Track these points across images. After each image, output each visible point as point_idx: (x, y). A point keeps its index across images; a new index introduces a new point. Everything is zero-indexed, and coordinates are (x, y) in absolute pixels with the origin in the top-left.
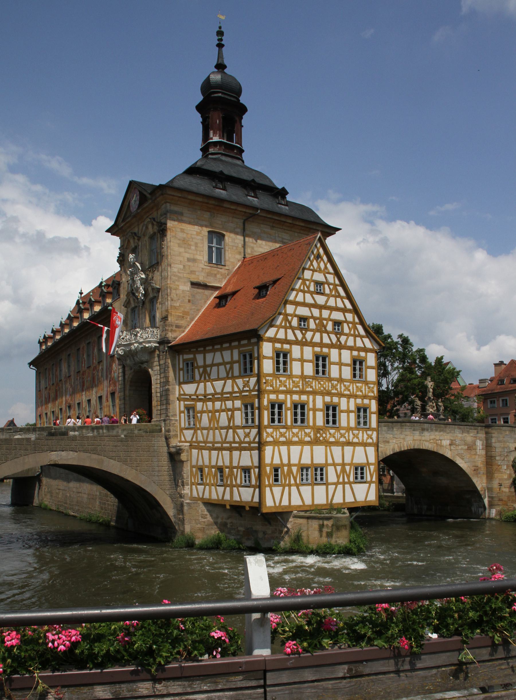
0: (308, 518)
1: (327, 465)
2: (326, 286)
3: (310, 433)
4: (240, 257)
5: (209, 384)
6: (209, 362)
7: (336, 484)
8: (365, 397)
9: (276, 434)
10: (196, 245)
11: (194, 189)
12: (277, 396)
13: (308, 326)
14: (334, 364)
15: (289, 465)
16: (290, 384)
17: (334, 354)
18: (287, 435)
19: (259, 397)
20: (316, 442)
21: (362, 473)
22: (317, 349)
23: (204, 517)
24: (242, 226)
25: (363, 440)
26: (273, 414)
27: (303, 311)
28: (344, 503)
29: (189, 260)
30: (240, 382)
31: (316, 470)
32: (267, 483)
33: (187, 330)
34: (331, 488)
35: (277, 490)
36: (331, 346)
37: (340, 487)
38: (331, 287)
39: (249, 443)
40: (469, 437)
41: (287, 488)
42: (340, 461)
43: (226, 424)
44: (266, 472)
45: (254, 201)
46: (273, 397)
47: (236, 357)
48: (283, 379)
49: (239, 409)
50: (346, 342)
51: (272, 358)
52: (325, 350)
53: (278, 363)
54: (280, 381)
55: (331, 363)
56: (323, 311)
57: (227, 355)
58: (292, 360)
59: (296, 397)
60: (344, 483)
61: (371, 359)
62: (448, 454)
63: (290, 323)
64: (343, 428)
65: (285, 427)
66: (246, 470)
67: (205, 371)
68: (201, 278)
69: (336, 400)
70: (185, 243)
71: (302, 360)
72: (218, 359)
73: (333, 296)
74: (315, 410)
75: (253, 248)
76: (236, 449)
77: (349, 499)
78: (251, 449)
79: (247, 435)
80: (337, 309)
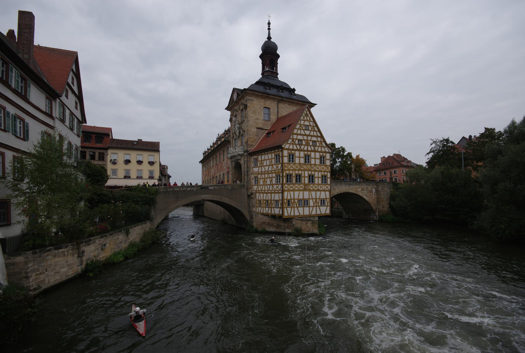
0: (302, 220)
4: (276, 117)
6: (263, 159)
7: (313, 207)
8: (325, 171)
9: (289, 187)
15: (294, 199)
16: (294, 167)
17: (313, 154)
19: (282, 172)
22: (306, 153)
26: (287, 179)
28: (316, 214)
29: (256, 119)
30: (275, 167)
35: (289, 209)
37: (315, 208)
39: (278, 190)
40: (370, 188)
46: (287, 172)
47: (273, 157)
52: (309, 153)
53: (290, 158)
55: (311, 158)
57: (270, 156)
58: (296, 157)
60: (316, 206)
61: (328, 156)
62: (360, 194)
67: (261, 163)
68: (261, 126)
69: (313, 173)
71: (299, 157)
72: (267, 158)
74: (304, 177)
76: (273, 193)
77: (319, 213)
78: (279, 193)
79: (277, 187)
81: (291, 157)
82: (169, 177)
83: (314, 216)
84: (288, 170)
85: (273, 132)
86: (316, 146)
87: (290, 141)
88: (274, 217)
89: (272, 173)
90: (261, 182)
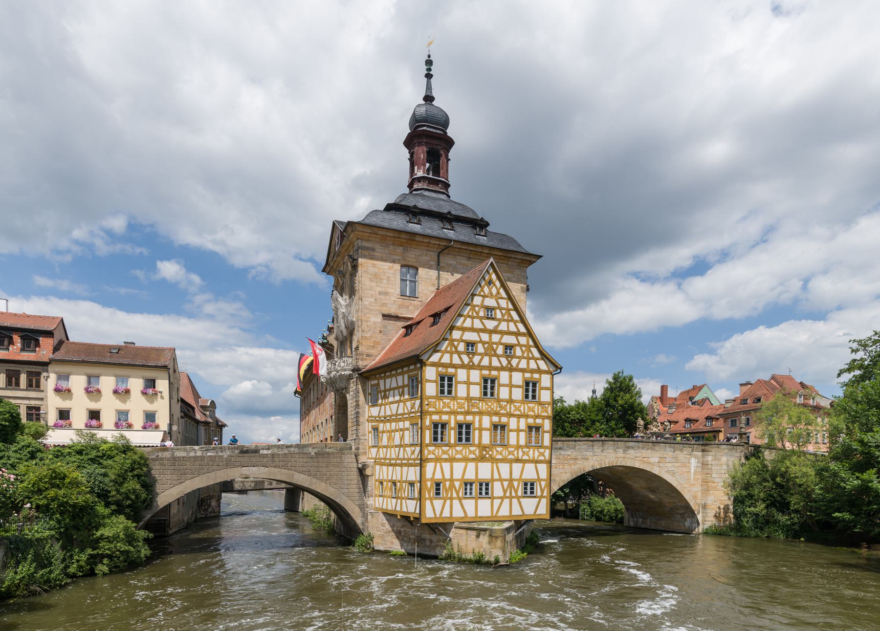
1: (493, 480)
2: (498, 311)
3: (475, 451)
5: (387, 406)
8: (537, 417)
9: (438, 452)
10: (388, 279)
11: (386, 225)
12: (440, 417)
13: (476, 349)
14: (504, 385)
15: (452, 480)
16: (454, 405)
17: (504, 377)
18: (450, 452)
20: (482, 459)
21: (532, 489)
22: (485, 372)
23: (383, 525)
24: (436, 259)
25: (534, 457)
26: (436, 433)
28: (511, 516)
31: (481, 485)
32: (427, 496)
33: (377, 359)
34: (497, 502)
35: (438, 503)
36: (502, 368)
38: (504, 312)
39: (414, 460)
41: (448, 502)
42: (508, 477)
43: (398, 443)
44: (426, 485)
45: (451, 234)
46: (435, 418)
47: (406, 382)
48: (447, 401)
49: (408, 429)
50: (518, 364)
51: (435, 381)
52: (494, 373)
53: (442, 386)
54: (444, 403)
55: (500, 385)
56: (494, 336)
59: (460, 418)
60: (511, 498)
62: (656, 471)
63: (456, 348)
64: (512, 446)
66: (412, 484)
68: (393, 311)
69: (504, 420)
70: (376, 277)
71: (468, 383)
73: (505, 320)
74: (481, 429)
75: (447, 280)
76: (406, 465)
77: (517, 511)
78: (415, 465)
79: (413, 453)
80: (509, 333)
81: (446, 383)
84: (437, 413)
85: (418, 323)
86: (514, 356)
89: (403, 420)
90: (385, 442)
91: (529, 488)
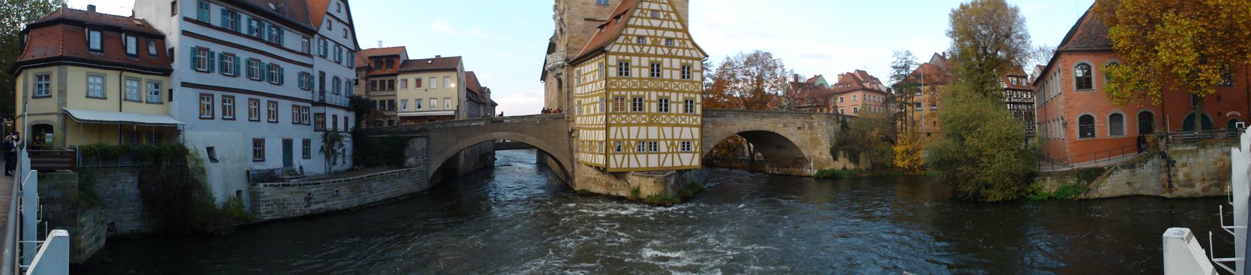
7: (667, 154)
9: (619, 119)
15: (629, 140)
16: (630, 84)
17: (666, 62)
20: (651, 124)
27: (641, 32)
34: (662, 156)
35: (619, 157)
36: (664, 56)
46: (616, 93)
52: (659, 59)
59: (635, 93)
65: (626, 113)
66: (601, 142)
69: (667, 94)
71: (640, 67)
74: (650, 101)
77: (677, 164)
82: (494, 105)
83: (668, 169)
87: (621, 39)
88: (598, 168)
91: (686, 146)
